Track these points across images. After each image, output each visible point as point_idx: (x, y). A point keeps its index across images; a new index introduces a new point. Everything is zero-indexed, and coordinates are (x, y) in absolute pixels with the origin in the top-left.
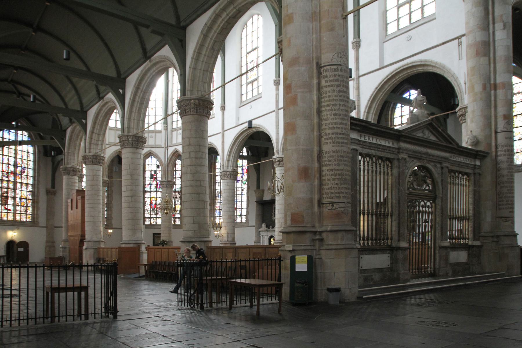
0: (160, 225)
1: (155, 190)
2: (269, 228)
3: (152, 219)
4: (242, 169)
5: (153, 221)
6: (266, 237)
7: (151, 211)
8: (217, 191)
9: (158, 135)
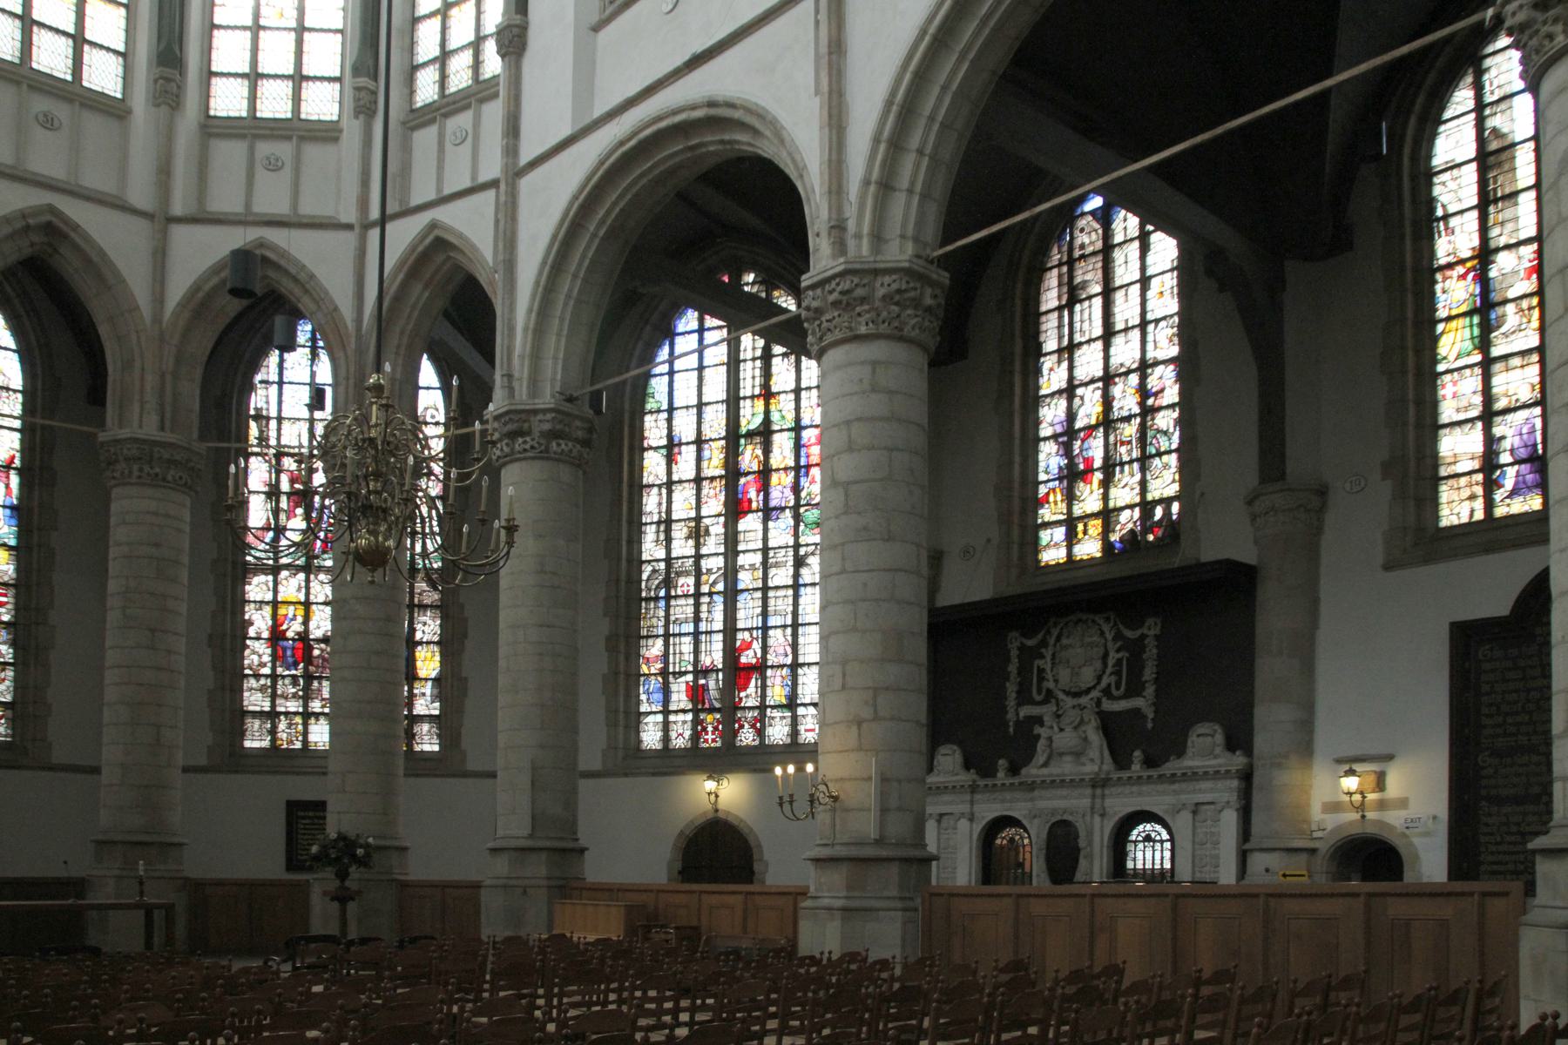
0: (322, 755)
2: (988, 771)
4: (798, 446)
6: (964, 824)
7: (274, 677)
8: (647, 570)
9: (313, 152)
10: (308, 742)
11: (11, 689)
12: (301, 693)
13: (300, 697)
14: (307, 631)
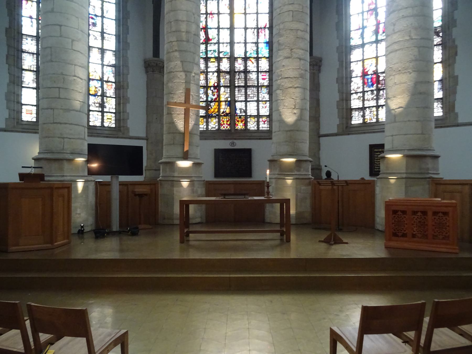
1: (374, 39)
3: (367, 112)
5: (370, 117)
7: (364, 92)
10: (378, 119)
11: (269, 110)
12: (375, 97)
13: (375, 99)
14: (377, 70)
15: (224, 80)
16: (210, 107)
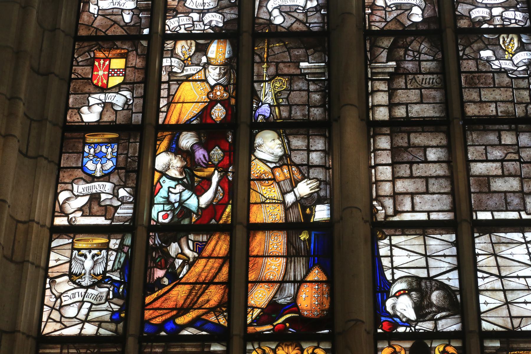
15: (280, 84)
16: (159, 273)
